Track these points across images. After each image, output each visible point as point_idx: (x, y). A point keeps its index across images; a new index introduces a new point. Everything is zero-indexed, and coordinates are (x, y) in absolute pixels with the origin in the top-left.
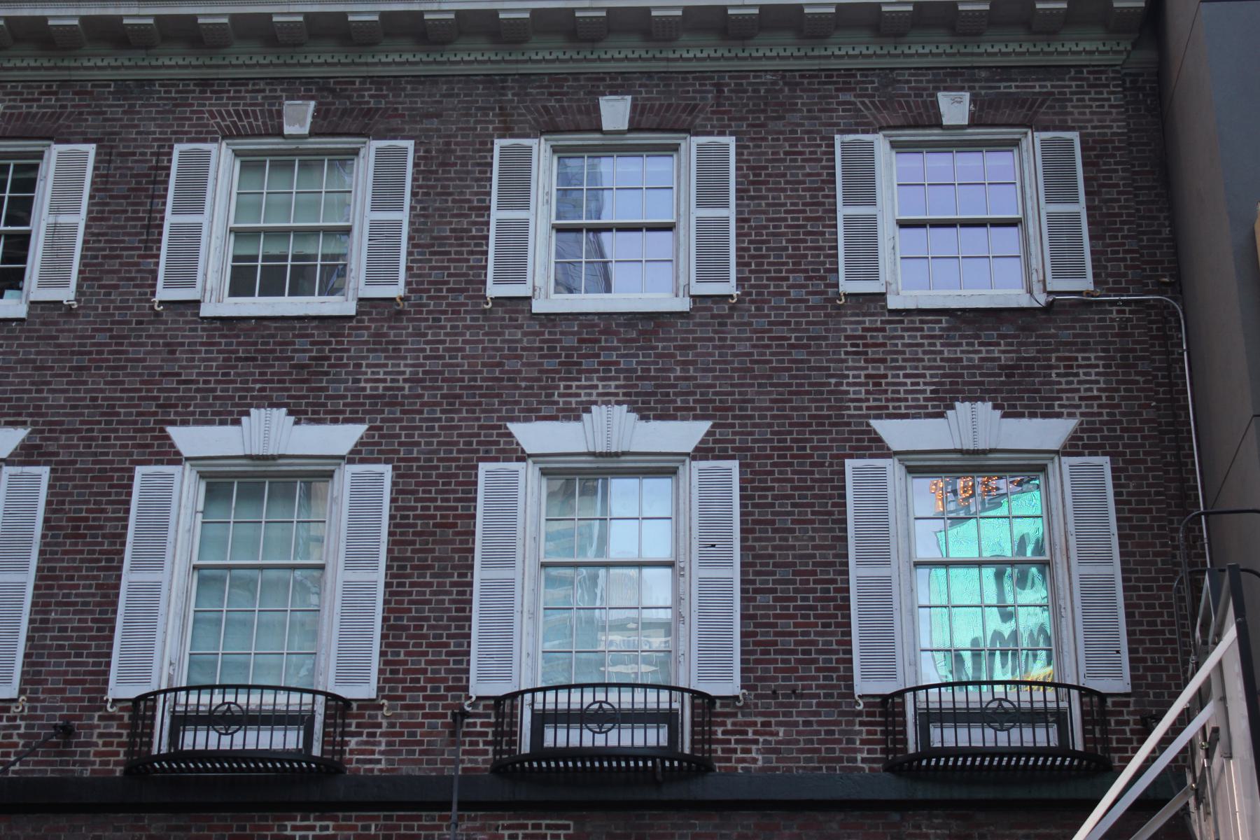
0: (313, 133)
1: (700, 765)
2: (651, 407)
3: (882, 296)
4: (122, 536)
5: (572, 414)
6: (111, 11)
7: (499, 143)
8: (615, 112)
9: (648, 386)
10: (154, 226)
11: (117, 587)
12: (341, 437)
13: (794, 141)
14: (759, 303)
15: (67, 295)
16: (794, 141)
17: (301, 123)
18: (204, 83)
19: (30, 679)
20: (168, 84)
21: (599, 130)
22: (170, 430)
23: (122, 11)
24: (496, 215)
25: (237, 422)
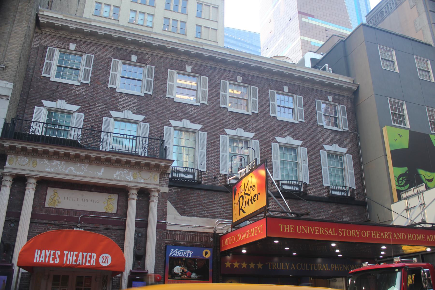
0: (242, 83)
1: (305, 194)
2: (295, 138)
3: (323, 126)
4: (219, 146)
5: (284, 137)
6: (214, 55)
7: (270, 90)
8: (286, 89)
9: (293, 134)
10: (219, 94)
11: (220, 155)
12: (251, 135)
13: (310, 99)
14: (308, 124)
15: (206, 103)
16: (310, 99)
17: (240, 80)
18: (224, 70)
19: (207, 169)
20: (219, 69)
21: (284, 91)
22: (225, 129)
23: (216, 56)
24: (271, 102)
25: (235, 130)
